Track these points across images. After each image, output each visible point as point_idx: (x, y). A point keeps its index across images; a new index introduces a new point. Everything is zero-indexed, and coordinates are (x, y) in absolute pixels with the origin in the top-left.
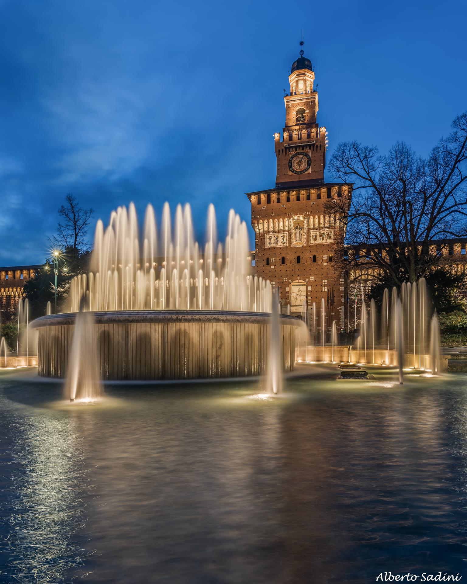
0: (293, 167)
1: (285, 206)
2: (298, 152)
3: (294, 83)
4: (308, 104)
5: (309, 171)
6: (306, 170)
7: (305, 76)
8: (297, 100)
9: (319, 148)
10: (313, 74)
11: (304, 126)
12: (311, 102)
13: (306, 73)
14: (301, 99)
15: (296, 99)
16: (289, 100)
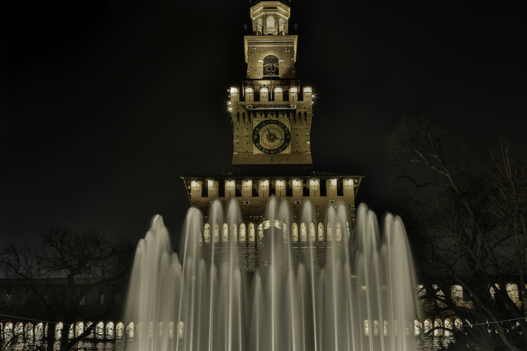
0: (261, 141)
1: (249, 203)
2: (268, 119)
3: (259, 18)
4: (284, 51)
5: (287, 151)
6: (283, 147)
7: (276, 11)
8: (266, 43)
9: (303, 117)
10: (289, 9)
11: (278, 82)
12: (286, 48)
13: (279, 8)
14: (271, 43)
15: (264, 41)
16: (252, 42)
